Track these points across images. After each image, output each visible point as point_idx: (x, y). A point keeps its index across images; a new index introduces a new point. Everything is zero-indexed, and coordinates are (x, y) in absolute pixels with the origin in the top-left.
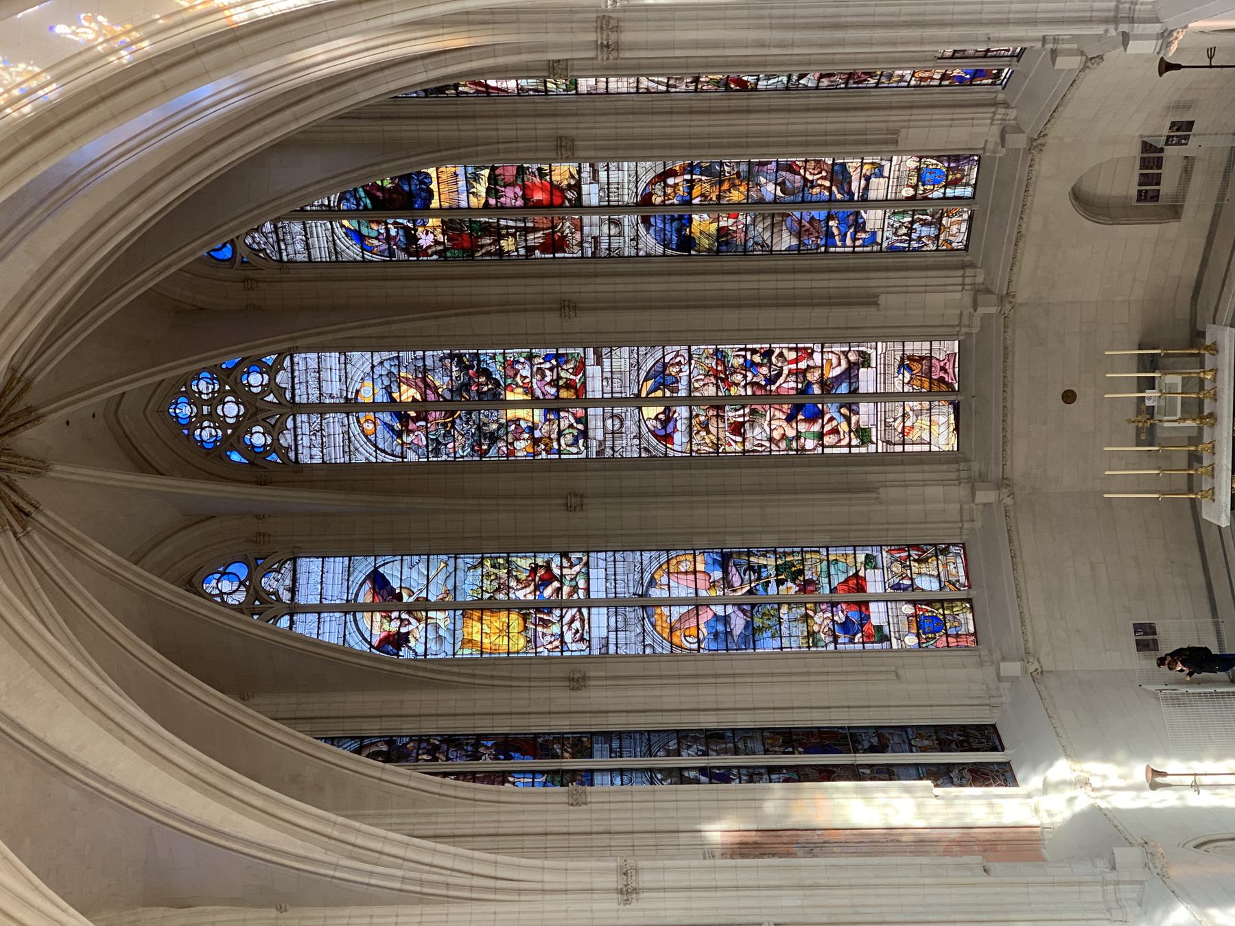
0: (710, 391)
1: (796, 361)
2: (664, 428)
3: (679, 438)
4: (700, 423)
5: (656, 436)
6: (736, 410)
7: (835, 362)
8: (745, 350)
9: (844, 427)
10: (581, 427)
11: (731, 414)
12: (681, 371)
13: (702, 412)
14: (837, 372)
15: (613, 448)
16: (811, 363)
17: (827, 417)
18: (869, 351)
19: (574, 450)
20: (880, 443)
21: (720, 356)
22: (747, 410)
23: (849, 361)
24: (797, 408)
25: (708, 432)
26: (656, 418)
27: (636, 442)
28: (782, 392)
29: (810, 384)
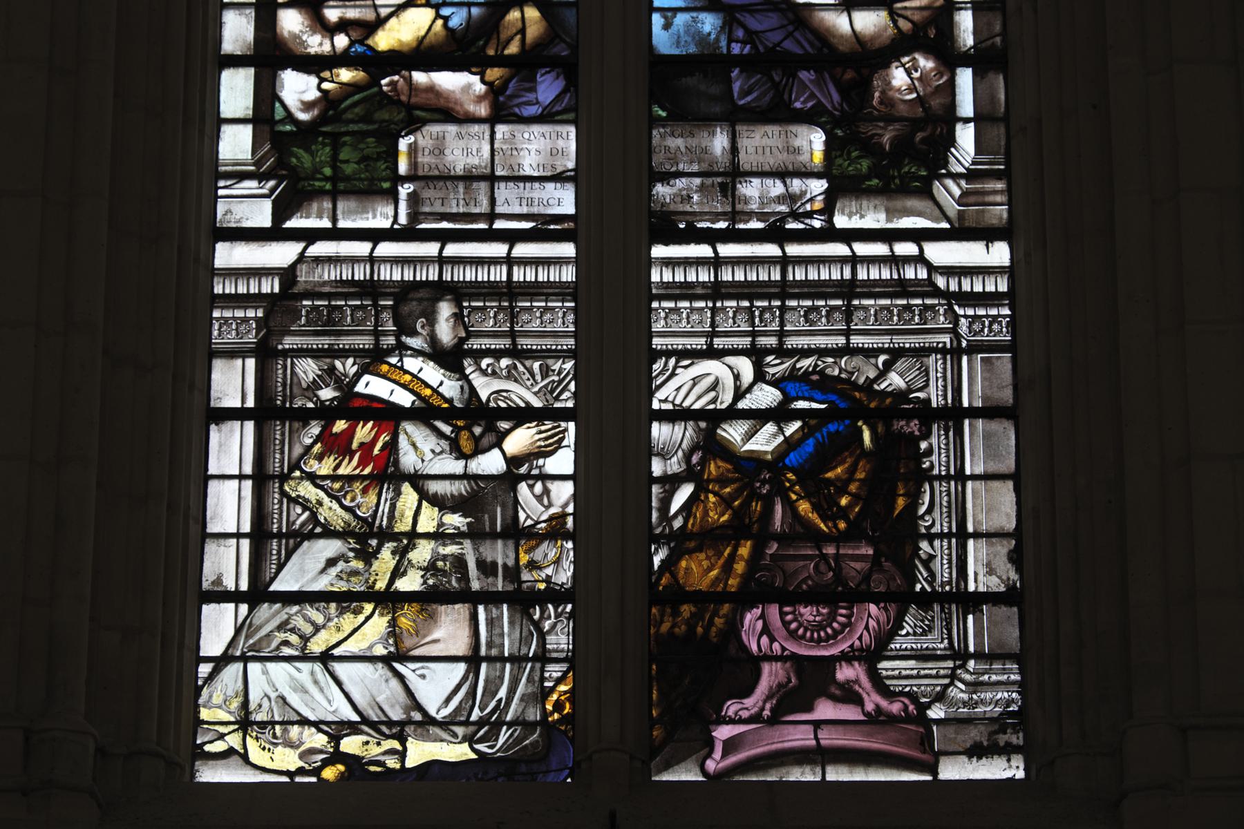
18: (948, 192)
20: (282, 254)
23: (871, 57)
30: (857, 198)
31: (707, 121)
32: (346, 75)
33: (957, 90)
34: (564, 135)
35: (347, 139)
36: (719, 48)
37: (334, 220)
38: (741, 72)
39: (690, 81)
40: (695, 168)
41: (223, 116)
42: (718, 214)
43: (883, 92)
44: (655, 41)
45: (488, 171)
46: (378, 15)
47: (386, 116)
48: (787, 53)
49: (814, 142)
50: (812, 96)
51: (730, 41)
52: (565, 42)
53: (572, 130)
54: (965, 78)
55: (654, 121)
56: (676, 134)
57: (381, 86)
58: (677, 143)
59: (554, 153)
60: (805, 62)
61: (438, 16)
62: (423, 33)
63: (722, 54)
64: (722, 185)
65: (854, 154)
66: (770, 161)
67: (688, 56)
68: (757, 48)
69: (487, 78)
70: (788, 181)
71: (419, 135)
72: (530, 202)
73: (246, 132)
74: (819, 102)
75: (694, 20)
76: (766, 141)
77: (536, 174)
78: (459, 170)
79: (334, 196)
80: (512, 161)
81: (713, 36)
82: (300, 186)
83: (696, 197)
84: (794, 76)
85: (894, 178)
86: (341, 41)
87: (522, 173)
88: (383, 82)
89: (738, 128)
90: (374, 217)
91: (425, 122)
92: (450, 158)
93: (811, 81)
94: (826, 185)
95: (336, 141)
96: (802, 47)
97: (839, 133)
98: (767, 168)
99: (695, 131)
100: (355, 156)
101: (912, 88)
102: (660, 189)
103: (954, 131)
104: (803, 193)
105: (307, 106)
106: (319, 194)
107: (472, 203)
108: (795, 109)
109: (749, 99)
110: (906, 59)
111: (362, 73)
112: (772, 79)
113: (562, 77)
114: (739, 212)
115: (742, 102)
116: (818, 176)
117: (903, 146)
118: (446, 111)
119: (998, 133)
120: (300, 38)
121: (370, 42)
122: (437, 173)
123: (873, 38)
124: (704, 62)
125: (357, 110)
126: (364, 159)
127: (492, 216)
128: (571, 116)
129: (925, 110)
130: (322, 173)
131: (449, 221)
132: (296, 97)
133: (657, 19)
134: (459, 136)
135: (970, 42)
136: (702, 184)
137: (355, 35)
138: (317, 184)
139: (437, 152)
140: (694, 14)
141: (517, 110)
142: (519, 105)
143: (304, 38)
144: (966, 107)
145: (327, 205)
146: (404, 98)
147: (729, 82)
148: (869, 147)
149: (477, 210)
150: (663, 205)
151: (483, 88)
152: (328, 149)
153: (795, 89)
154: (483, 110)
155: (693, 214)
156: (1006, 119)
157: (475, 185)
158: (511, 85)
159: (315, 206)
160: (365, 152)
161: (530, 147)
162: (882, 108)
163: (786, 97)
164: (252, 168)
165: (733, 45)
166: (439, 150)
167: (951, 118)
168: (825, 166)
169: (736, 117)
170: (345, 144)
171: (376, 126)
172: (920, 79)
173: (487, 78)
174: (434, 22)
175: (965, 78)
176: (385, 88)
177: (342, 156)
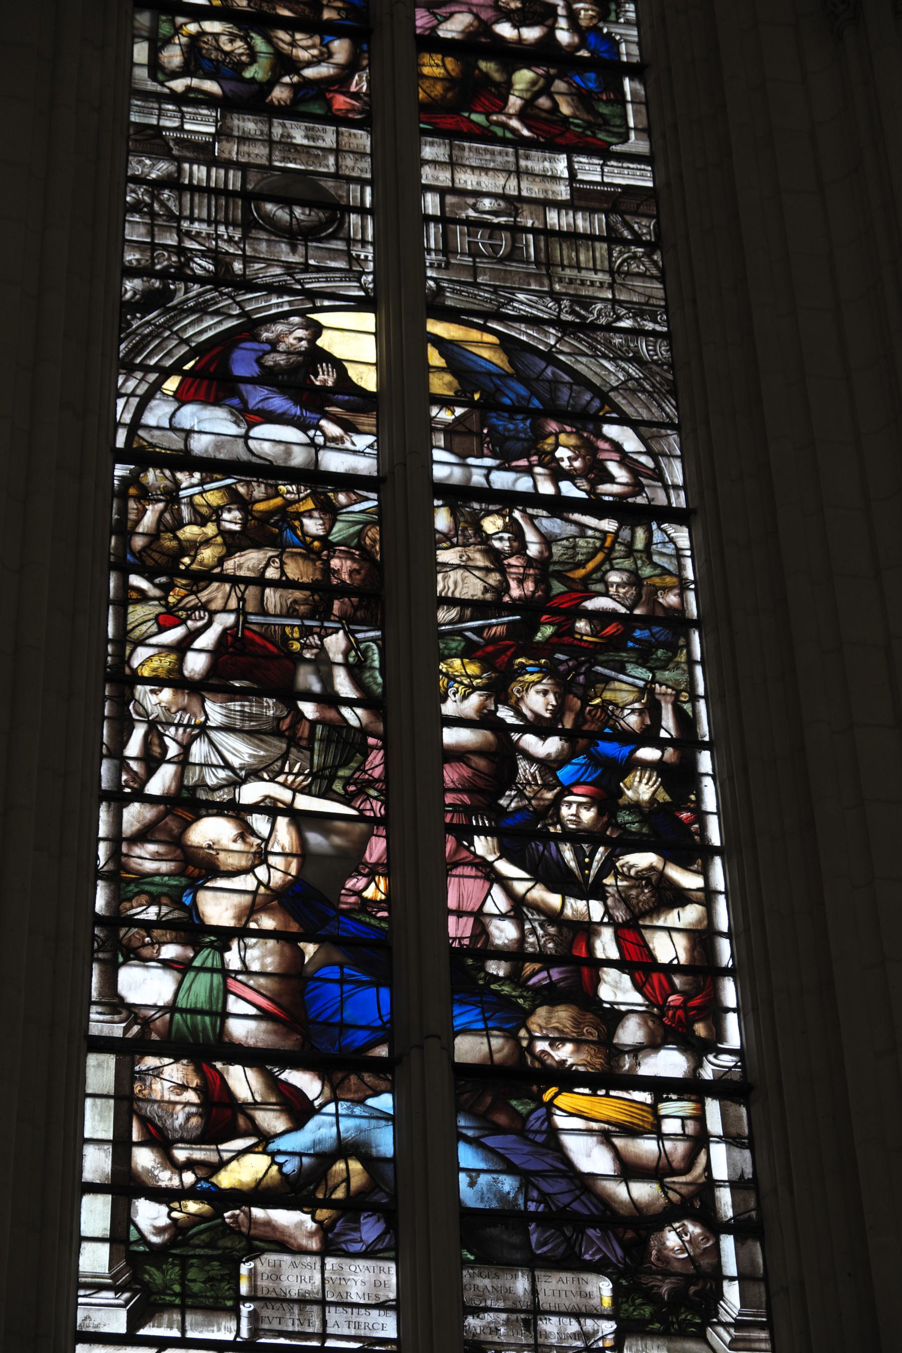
0: (460, 577)
1: (638, 963)
2: (269, 378)
3: (210, 426)
4: (287, 516)
5: (225, 343)
6: (356, 672)
7: (647, 1147)
8: (687, 741)
9: (245, 1170)
10: (280, 94)
11: (336, 644)
12: (558, 474)
13: (339, 531)
14: (590, 1157)
15: (172, 182)
16: (631, 1033)
17: (308, 1084)
19: (173, 56)
21: (650, 634)
22: (353, 716)
23: (646, 1223)
24: (368, 947)
25: (234, 543)
26: (317, 356)
27: (202, 266)
28: (461, 890)
29: (506, 1014)
30: (642, 1338)
31: (511, 1266)
32: (193, 1207)
33: (722, 1253)
34: (386, 1270)
35: (194, 1261)
36: (517, 1205)
37: (183, 1330)
38: (537, 1226)
39: (495, 1231)
40: (501, 1305)
41: (83, 1234)
42: (522, 1345)
43: (659, 1251)
44: (462, 1195)
45: (320, 1296)
46: (221, 1158)
47: (229, 1244)
48: (575, 1212)
49: (603, 1289)
50: (599, 1250)
51: (526, 1200)
52: (382, 1190)
53: (393, 1266)
54: (728, 1243)
55: (465, 1263)
56: (483, 1275)
57: (224, 1218)
58: (485, 1282)
59: (377, 1284)
60: (593, 1222)
61: (274, 1162)
62: (260, 1175)
63: (520, 1211)
64: (524, 1320)
65: (638, 1301)
66: (567, 1303)
67: (491, 1210)
68: (550, 1208)
69: (317, 1217)
70: (582, 1321)
71: (258, 1261)
72: (357, 1326)
73: (105, 1248)
74: (605, 1255)
75: (495, 1180)
76: (561, 1286)
77: (362, 1302)
78: (294, 1294)
79: (183, 1310)
80: (341, 1290)
81: (512, 1195)
82: (152, 1299)
83: (502, 1330)
84: (583, 1233)
85: (673, 1323)
86: (189, 1178)
87: (349, 1300)
88: (226, 1215)
89: (537, 1273)
90: (219, 1330)
91: (263, 1251)
92: (285, 1283)
93: (598, 1238)
94: (615, 1326)
95: (184, 1263)
96: (589, 1209)
97: (624, 1282)
98: (563, 1309)
99: (500, 1273)
100: (202, 1276)
101: (683, 1249)
102: (471, 1321)
103: (722, 1287)
104: (596, 1332)
105: (159, 1231)
106: (170, 1307)
107: (306, 1323)
108: (585, 1260)
109: (545, 1249)
110: (676, 1225)
111: (207, 1207)
112: (564, 1234)
113: (382, 1221)
114: (541, 1345)
115: (539, 1252)
116: (608, 1318)
117: (679, 1298)
118: (281, 1243)
119: (760, 1290)
120: (152, 1173)
121: (214, 1180)
122: (274, 1295)
123: (649, 1205)
124: (504, 1216)
125: (203, 1237)
126: (210, 1279)
127: (324, 1336)
128: (392, 1254)
129: (696, 1267)
130: (171, 1289)
131: (286, 1337)
132: (149, 1222)
133: (463, 1178)
134: (294, 1265)
135: (730, 1213)
136: (508, 1319)
137: (201, 1173)
138: (167, 1298)
139: (274, 1277)
140: (495, 1176)
141: (344, 1246)
142: (345, 1242)
143: (156, 1173)
144: (730, 1266)
145: (177, 1317)
146: (244, 1230)
147: (527, 1234)
148: (650, 1296)
149: (310, 1330)
150: (474, 1335)
151: (314, 1225)
152: (177, 1269)
153: (584, 1244)
154: (314, 1244)
155: (501, 1344)
156: (765, 1279)
157: (308, 1308)
158: (338, 1224)
159: (166, 1317)
160: (211, 1273)
161: (356, 1278)
162: (659, 1264)
163: (577, 1249)
164: (110, 1281)
165: (529, 1203)
166: (276, 1276)
167: (718, 1276)
168: (613, 1310)
169: (534, 1264)
170: (192, 1265)
171: (220, 1252)
172: (690, 1242)
173: (317, 1217)
174: (270, 1167)
175: (728, 1243)
176: (227, 1220)
177: (190, 1276)
